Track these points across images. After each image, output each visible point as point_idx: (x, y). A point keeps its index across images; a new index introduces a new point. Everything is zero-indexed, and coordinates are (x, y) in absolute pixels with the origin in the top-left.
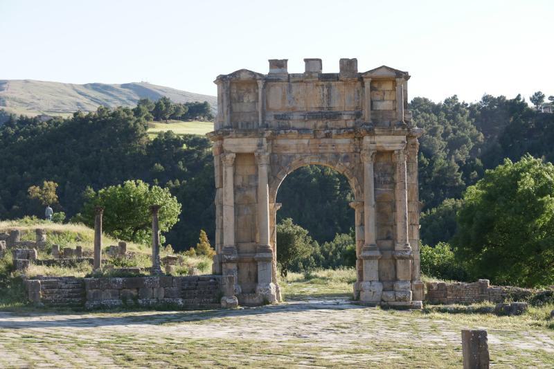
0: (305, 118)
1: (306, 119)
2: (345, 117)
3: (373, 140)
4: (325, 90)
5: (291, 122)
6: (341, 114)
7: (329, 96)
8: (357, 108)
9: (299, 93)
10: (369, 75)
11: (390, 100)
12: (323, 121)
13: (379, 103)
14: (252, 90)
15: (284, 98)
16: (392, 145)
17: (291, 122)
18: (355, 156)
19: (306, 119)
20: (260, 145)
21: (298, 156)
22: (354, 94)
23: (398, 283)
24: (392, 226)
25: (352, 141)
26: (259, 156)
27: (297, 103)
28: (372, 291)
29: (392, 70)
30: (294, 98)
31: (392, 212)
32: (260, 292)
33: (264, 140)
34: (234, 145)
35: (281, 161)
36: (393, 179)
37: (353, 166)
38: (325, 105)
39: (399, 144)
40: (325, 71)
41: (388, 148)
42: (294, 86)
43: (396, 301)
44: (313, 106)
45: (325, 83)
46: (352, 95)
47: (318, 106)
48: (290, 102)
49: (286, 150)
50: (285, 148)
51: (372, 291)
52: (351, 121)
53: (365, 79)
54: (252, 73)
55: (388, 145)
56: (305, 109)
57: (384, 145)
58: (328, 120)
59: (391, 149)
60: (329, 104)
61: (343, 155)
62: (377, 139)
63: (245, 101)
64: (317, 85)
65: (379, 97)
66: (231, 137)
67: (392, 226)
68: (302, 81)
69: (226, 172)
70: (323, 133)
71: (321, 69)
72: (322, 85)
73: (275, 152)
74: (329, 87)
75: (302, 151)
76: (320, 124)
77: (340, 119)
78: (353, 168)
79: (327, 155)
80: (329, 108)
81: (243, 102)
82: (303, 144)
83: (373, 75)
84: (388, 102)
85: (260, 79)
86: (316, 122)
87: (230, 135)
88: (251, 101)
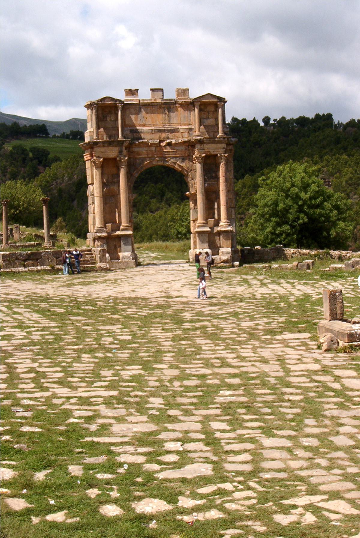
1: (153, 132)
10: (198, 100)
11: (213, 118)
13: (205, 120)
14: (113, 112)
19: (153, 132)
20: (121, 152)
25: (187, 147)
26: (120, 160)
33: (124, 148)
34: (102, 152)
39: (221, 150)
41: (213, 152)
49: (139, 155)
50: (138, 154)
52: (186, 133)
53: (195, 103)
54: (113, 99)
55: (213, 150)
57: (210, 150)
58: (169, 133)
59: (215, 153)
60: (169, 121)
63: (108, 120)
64: (160, 108)
65: (205, 116)
66: (99, 147)
72: (164, 108)
75: (150, 156)
76: (163, 135)
77: (178, 132)
81: (106, 120)
82: (152, 151)
84: (211, 120)
86: (160, 134)
87: (98, 145)
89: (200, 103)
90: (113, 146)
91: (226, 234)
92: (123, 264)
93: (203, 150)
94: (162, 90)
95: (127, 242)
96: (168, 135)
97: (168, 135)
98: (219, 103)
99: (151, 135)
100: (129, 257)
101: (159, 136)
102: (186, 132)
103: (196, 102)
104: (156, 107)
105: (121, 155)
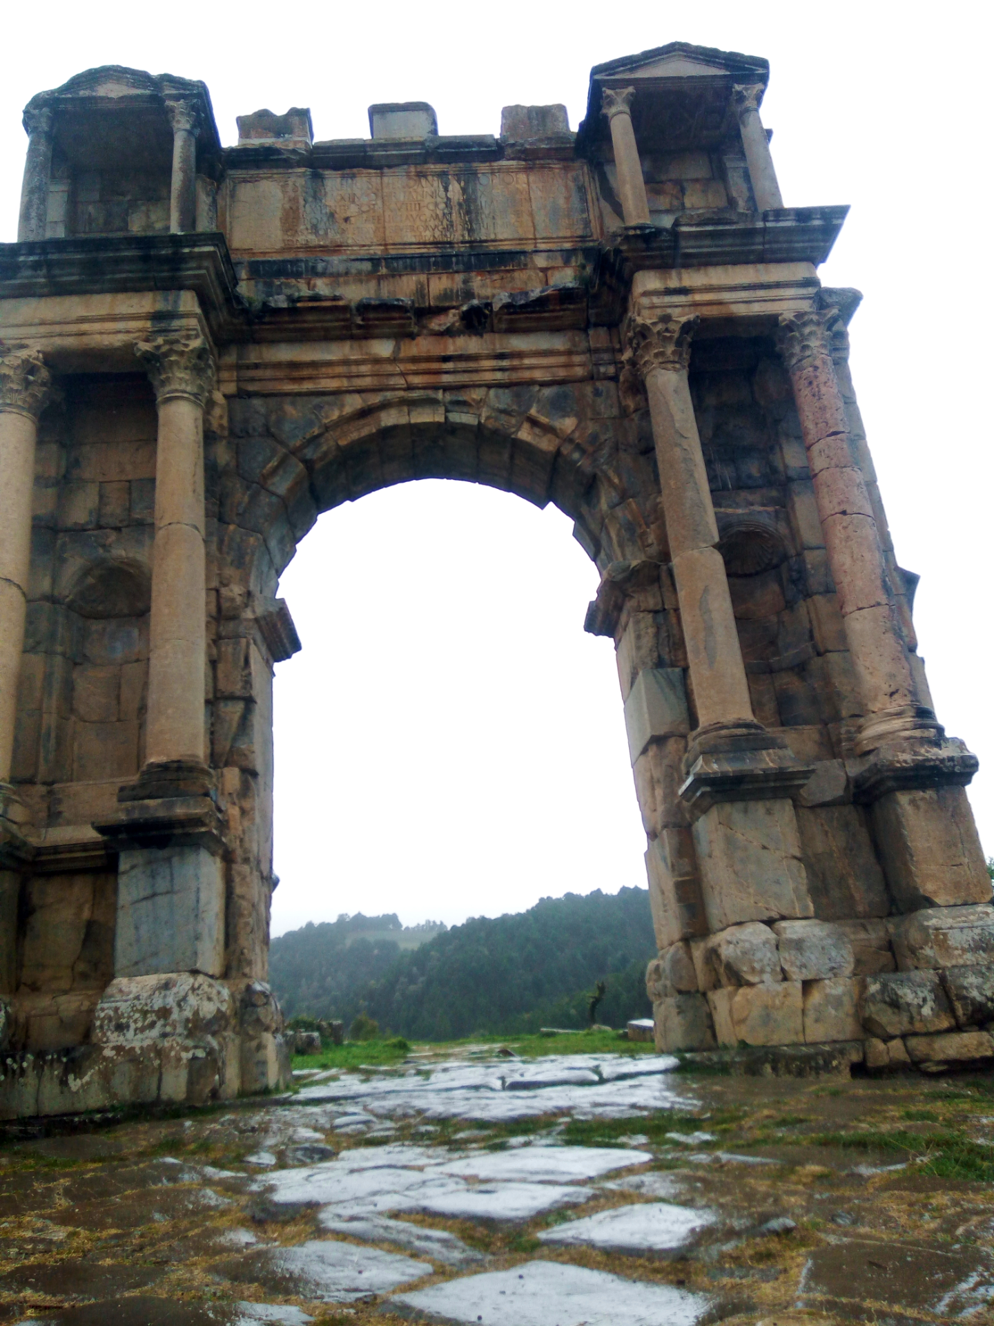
3: (673, 283)
4: (455, 189)
6: (524, 253)
7: (469, 207)
15: (291, 219)
16: (761, 293)
18: (597, 393)
19: (383, 271)
21: (354, 403)
22: (567, 199)
23: (935, 919)
24: (801, 669)
27: (343, 231)
28: (793, 971)
29: (709, 56)
31: (790, 605)
32: (115, 1038)
33: (188, 302)
35: (279, 421)
36: (774, 470)
37: (591, 427)
40: (449, 127)
43: (957, 1028)
45: (451, 168)
46: (561, 202)
47: (428, 236)
51: (798, 976)
54: (141, 78)
57: (726, 296)
59: (757, 309)
60: (470, 231)
64: (421, 175)
67: (801, 669)
72: (442, 175)
73: (251, 387)
76: (439, 285)
78: (594, 438)
83: (641, 74)
85: (177, 98)
86: (423, 278)
89: (631, 89)
91: (929, 794)
92: (106, 1076)
94: (424, 108)
95: (162, 885)
97: (465, 282)
100: (164, 1013)
101: (413, 286)
103: (615, 85)
104: (400, 171)
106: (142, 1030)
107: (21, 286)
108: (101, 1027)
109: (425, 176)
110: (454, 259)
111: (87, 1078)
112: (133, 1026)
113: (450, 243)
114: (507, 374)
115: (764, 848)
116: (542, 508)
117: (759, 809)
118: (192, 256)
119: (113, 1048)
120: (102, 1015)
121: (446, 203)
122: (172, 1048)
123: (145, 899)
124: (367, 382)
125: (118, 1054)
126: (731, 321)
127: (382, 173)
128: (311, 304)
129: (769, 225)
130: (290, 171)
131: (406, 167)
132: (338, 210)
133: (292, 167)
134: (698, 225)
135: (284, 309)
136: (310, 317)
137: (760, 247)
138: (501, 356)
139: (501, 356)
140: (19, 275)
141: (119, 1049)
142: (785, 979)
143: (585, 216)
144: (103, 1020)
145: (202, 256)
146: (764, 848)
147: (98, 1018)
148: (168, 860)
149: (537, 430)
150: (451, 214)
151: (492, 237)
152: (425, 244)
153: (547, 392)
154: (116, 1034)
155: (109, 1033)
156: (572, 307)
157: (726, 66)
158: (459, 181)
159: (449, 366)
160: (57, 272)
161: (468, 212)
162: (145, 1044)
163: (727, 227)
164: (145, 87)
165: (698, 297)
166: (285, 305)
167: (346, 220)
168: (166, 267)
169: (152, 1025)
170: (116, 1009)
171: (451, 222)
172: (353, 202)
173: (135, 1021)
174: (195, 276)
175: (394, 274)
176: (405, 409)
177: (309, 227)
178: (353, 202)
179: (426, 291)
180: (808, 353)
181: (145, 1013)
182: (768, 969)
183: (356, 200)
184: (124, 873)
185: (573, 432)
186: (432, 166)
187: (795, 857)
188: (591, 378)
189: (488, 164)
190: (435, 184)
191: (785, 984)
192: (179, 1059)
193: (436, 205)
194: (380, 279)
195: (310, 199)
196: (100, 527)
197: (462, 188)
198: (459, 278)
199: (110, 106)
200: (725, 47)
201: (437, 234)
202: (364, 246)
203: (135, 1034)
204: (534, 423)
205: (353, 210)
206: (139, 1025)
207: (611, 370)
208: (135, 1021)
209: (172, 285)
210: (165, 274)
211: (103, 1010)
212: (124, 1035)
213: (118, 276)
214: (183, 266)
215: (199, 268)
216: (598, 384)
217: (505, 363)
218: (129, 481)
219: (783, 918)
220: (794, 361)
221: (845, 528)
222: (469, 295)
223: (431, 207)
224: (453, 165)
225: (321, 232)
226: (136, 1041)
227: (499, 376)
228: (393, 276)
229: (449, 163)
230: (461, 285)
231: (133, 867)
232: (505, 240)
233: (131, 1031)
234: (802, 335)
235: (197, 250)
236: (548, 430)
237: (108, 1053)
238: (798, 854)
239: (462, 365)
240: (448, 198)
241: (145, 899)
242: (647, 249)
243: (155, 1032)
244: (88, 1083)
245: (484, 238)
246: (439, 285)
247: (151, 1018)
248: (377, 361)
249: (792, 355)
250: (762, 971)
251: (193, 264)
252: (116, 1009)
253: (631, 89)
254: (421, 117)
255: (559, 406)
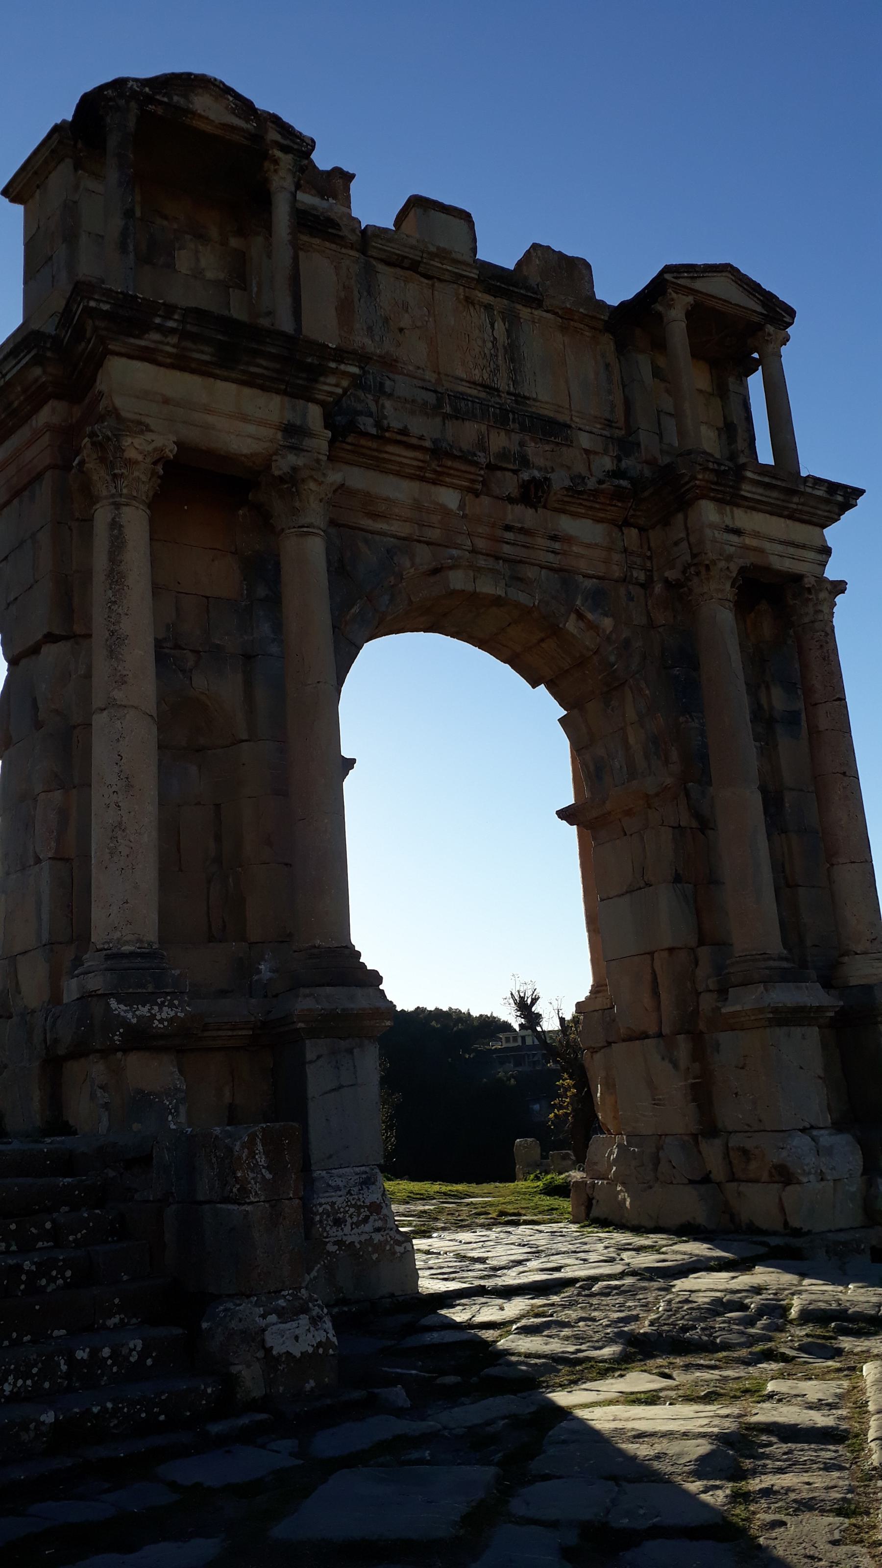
0: (439, 405)
1: (448, 409)
2: (585, 441)
4: (500, 327)
5: (388, 404)
7: (512, 352)
8: (609, 423)
9: (406, 307)
12: (508, 432)
15: (345, 309)
16: (791, 550)
17: (388, 404)
21: (424, 556)
27: (399, 345)
29: (753, 288)
30: (386, 320)
33: (314, 414)
34: (166, 401)
38: (502, 383)
42: (386, 276)
44: (460, 373)
47: (477, 375)
48: (370, 329)
49: (375, 516)
54: (245, 107)
55: (779, 548)
56: (430, 376)
57: (767, 546)
59: (788, 566)
60: (515, 382)
61: (588, 583)
62: (742, 518)
63: (184, 261)
66: (147, 356)
68: (414, 267)
69: (115, 525)
70: (509, 484)
71: (474, 250)
72: (488, 307)
74: (512, 320)
76: (499, 441)
78: (627, 643)
79: (531, 573)
80: (520, 399)
83: (698, 285)
85: (285, 149)
88: (209, 275)
89: (690, 299)
90: (250, 382)
93: (734, 538)
96: (522, 444)
97: (522, 444)
98: (770, 328)
99: (438, 420)
102: (606, 452)
105: (296, 449)
106: (357, 1224)
107: (146, 348)
108: (321, 1221)
109: (473, 304)
110: (511, 416)
111: (314, 1273)
112: (349, 1220)
113: (497, 390)
114: (559, 557)
115: (801, 1068)
116: (534, 687)
117: (797, 1031)
118: (334, 372)
119: (335, 1243)
120: (321, 1210)
121: (493, 343)
122: (387, 1242)
123: (333, 1090)
124: (434, 534)
125: (340, 1249)
126: (767, 569)
127: (433, 285)
128: (399, 437)
129: (809, 490)
130: (343, 251)
131: (455, 286)
132: (392, 316)
133: (346, 247)
134: (760, 474)
135: (372, 435)
136: (390, 448)
137: (795, 506)
138: (554, 538)
139: (554, 538)
140: (146, 336)
141: (339, 1243)
142: (822, 1180)
143: (611, 398)
144: (321, 1214)
145: (345, 374)
146: (801, 1068)
147: (316, 1214)
148: (350, 1051)
149: (581, 624)
150: (496, 356)
151: (535, 396)
152: (474, 383)
153: (588, 583)
154: (334, 1229)
155: (328, 1228)
156: (620, 504)
157: (764, 305)
158: (503, 320)
159: (509, 536)
160: (188, 344)
161: (512, 360)
162: (363, 1238)
163: (779, 483)
164: (247, 121)
165: (748, 541)
166: (373, 431)
167: (401, 330)
168: (304, 375)
169: (366, 1220)
170: (334, 1203)
171: (498, 366)
172: (407, 311)
173: (351, 1217)
174: (331, 394)
175: (458, 416)
176: (471, 574)
177: (365, 328)
178: (407, 311)
179: (487, 444)
180: (820, 617)
181: (358, 1208)
182: (813, 1171)
183: (410, 310)
184: (311, 1062)
185: (611, 632)
186: (480, 295)
187: (820, 1077)
188: (624, 580)
189: (529, 310)
190: (483, 317)
191: (823, 1183)
192: (394, 1253)
193: (484, 342)
194: (446, 417)
195: (365, 294)
196: (177, 647)
197: (507, 331)
198: (516, 437)
199: (208, 128)
200: (767, 286)
201: (486, 376)
202: (419, 368)
203: (352, 1229)
204: (580, 616)
205: (405, 321)
206: (355, 1219)
207: (642, 576)
208: (351, 1217)
209: (303, 394)
210: (300, 382)
211: (321, 1205)
212: (342, 1229)
213: (253, 369)
214: (322, 379)
215: (337, 385)
216: (630, 587)
217: (557, 546)
218: (207, 598)
219: (812, 1127)
220: (806, 620)
221: (844, 788)
222: (525, 462)
223: (480, 343)
224: (499, 299)
225: (377, 338)
226: (352, 1235)
227: (551, 557)
228: (457, 418)
229: (495, 297)
230: (517, 448)
231: (319, 1057)
232: (547, 403)
233: (348, 1226)
234: (817, 599)
235: (342, 367)
236: (592, 627)
237: (331, 1248)
238: (822, 1075)
239: (521, 538)
240: (495, 338)
241: (333, 1090)
242: (716, 483)
243: (368, 1228)
244: (315, 1278)
245: (527, 394)
246: (499, 441)
247: (365, 1212)
248: (445, 511)
249: (807, 614)
250: (809, 1173)
251: (332, 380)
252: (334, 1203)
253: (690, 299)
254: (459, 224)
255: (597, 598)
